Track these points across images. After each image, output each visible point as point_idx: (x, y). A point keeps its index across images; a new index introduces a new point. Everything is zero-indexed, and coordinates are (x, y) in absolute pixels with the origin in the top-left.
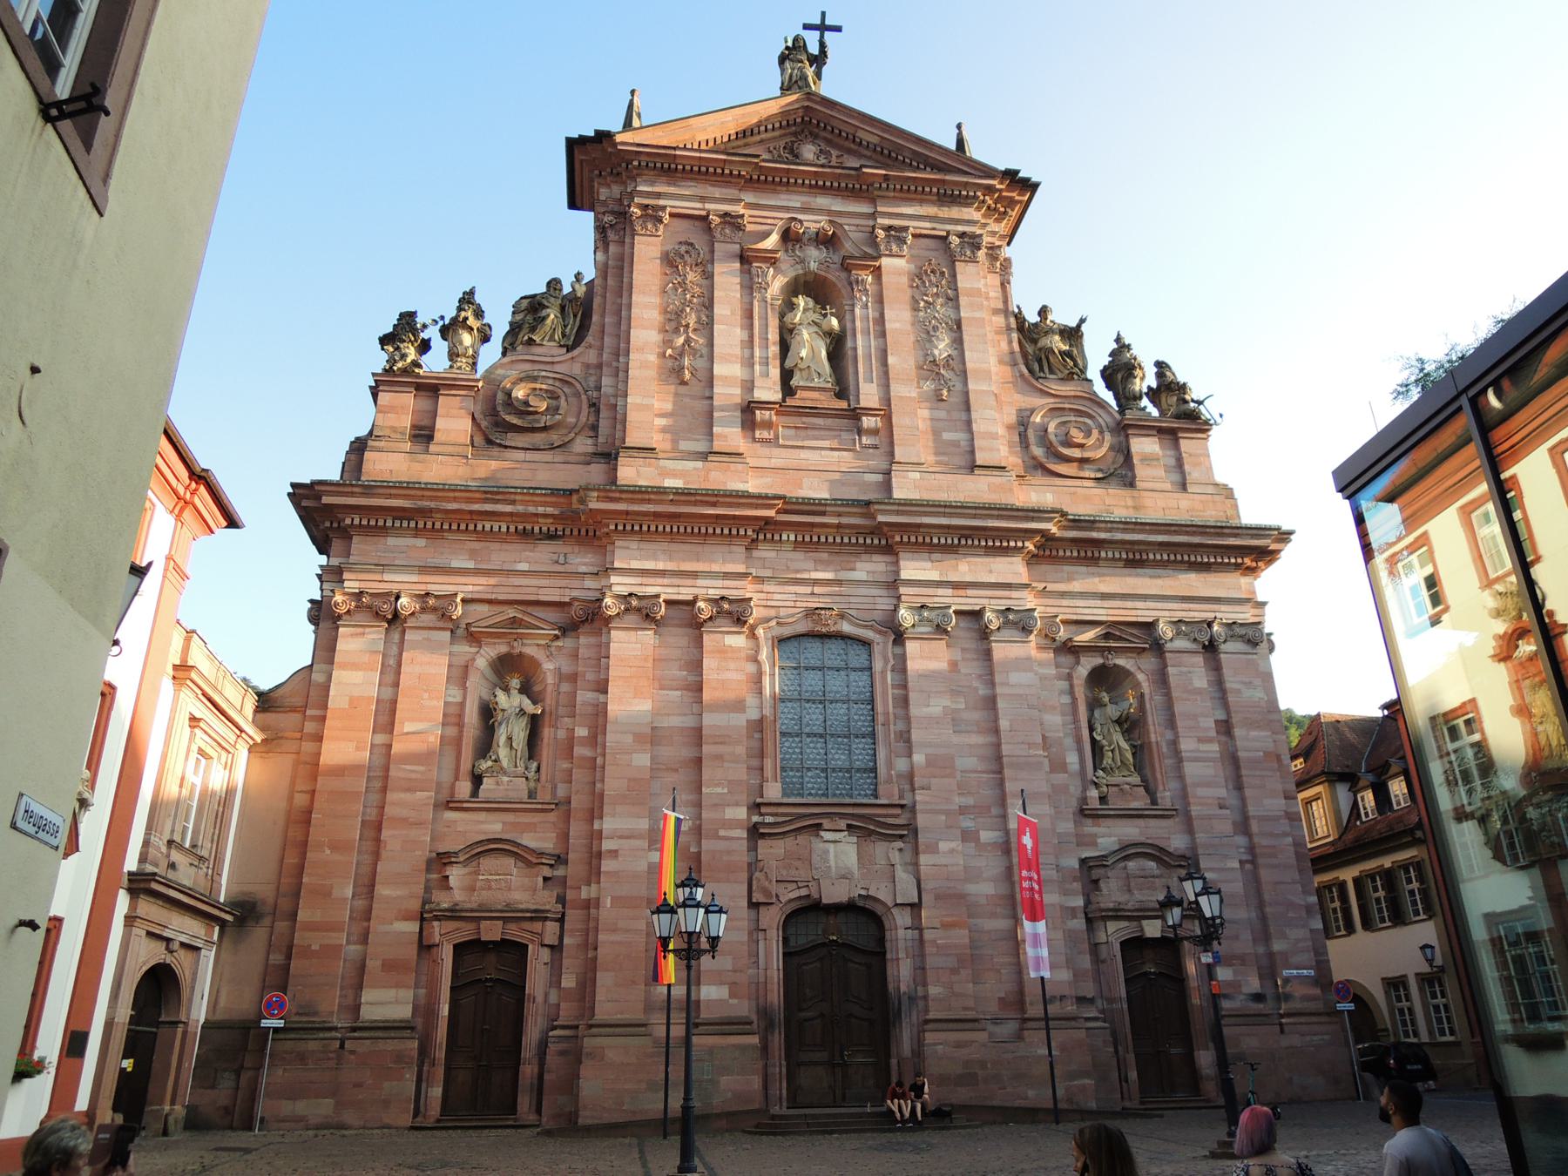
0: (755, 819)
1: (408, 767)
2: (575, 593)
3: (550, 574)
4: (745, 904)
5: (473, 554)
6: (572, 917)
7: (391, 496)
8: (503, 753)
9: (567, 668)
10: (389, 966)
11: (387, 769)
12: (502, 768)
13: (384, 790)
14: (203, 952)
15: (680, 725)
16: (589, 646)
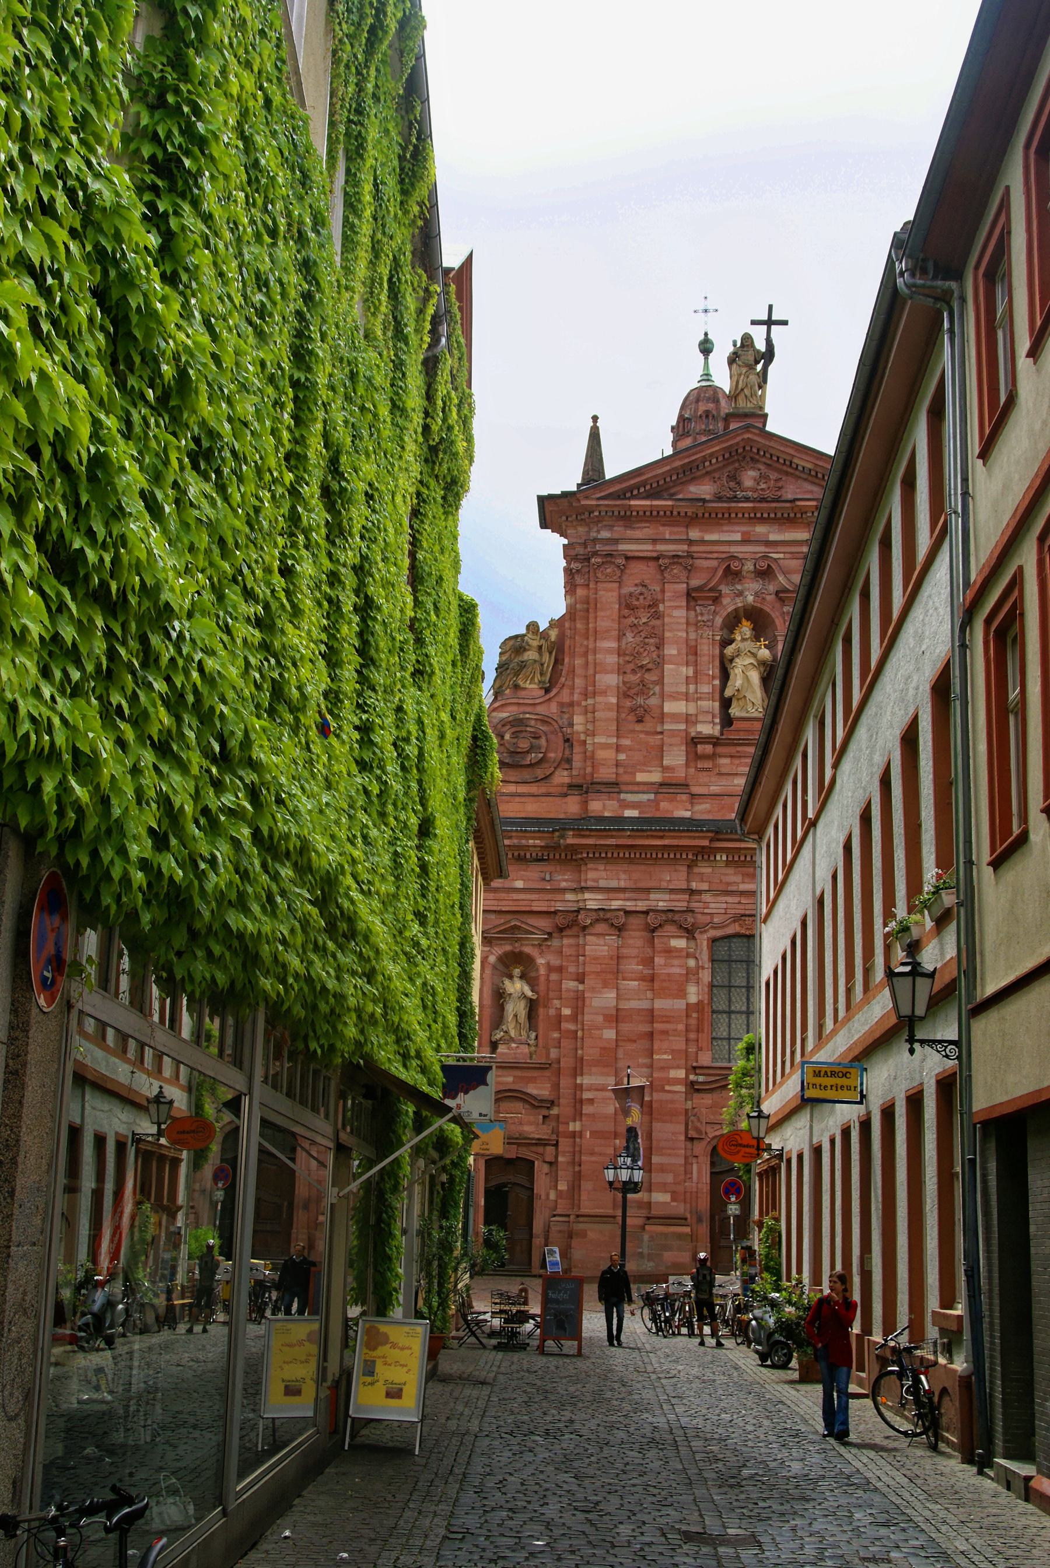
0: (692, 1077)
4: (683, 1138)
6: (564, 1144)
9: (555, 961)
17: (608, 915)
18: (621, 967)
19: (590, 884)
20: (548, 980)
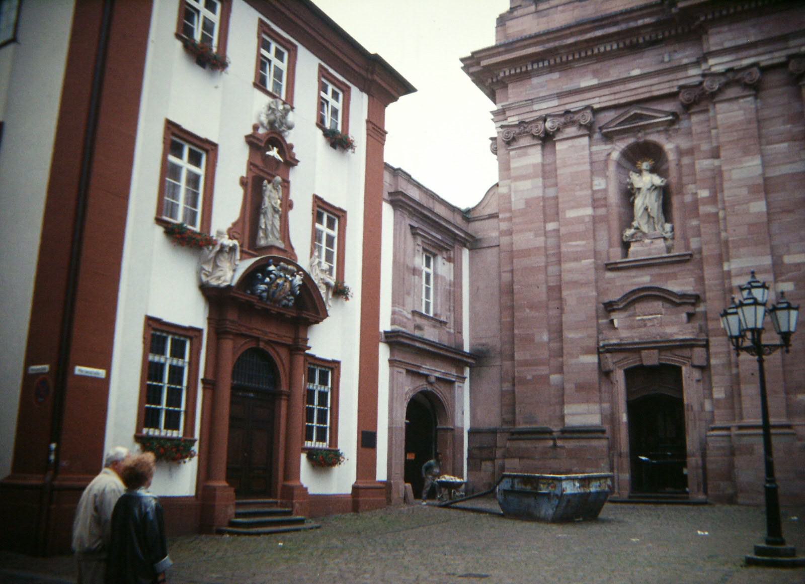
1: (574, 243)
2: (682, 83)
3: (657, 73)
5: (595, 74)
7: (525, 47)
8: (640, 221)
9: (684, 144)
10: (580, 387)
11: (559, 247)
12: (644, 234)
13: (559, 262)
14: (457, 384)
15: (790, 172)
16: (700, 123)
17: (739, 76)
18: (764, 131)
19: (713, 49)
20: (679, 165)
